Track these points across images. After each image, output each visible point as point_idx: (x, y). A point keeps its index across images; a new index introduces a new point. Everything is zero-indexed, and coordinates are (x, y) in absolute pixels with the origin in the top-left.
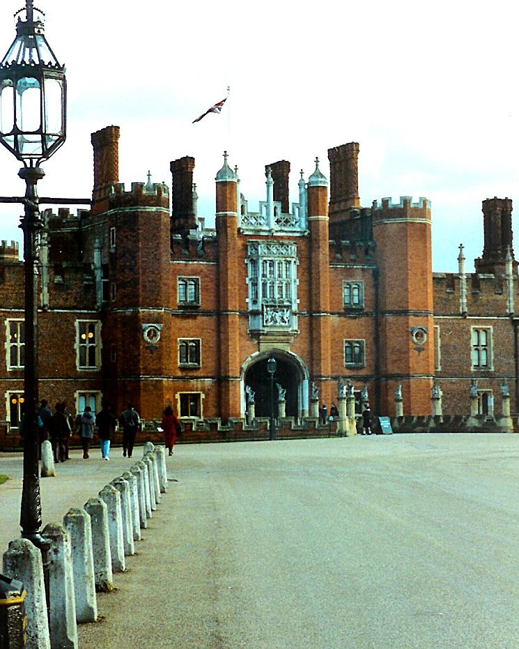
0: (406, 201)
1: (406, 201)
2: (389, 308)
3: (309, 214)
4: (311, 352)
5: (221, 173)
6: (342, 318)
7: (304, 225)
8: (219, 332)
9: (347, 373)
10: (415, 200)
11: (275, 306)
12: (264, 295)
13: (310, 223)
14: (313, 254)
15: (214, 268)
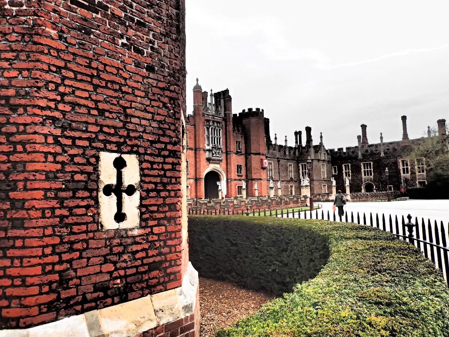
0: (258, 109)
1: (258, 109)
2: (252, 152)
3: (225, 111)
4: (227, 168)
5: (195, 88)
6: (236, 155)
7: (223, 115)
8: (196, 158)
9: (238, 178)
10: (261, 111)
11: (216, 148)
12: (212, 143)
13: (225, 114)
14: (228, 127)
15: (193, 129)
